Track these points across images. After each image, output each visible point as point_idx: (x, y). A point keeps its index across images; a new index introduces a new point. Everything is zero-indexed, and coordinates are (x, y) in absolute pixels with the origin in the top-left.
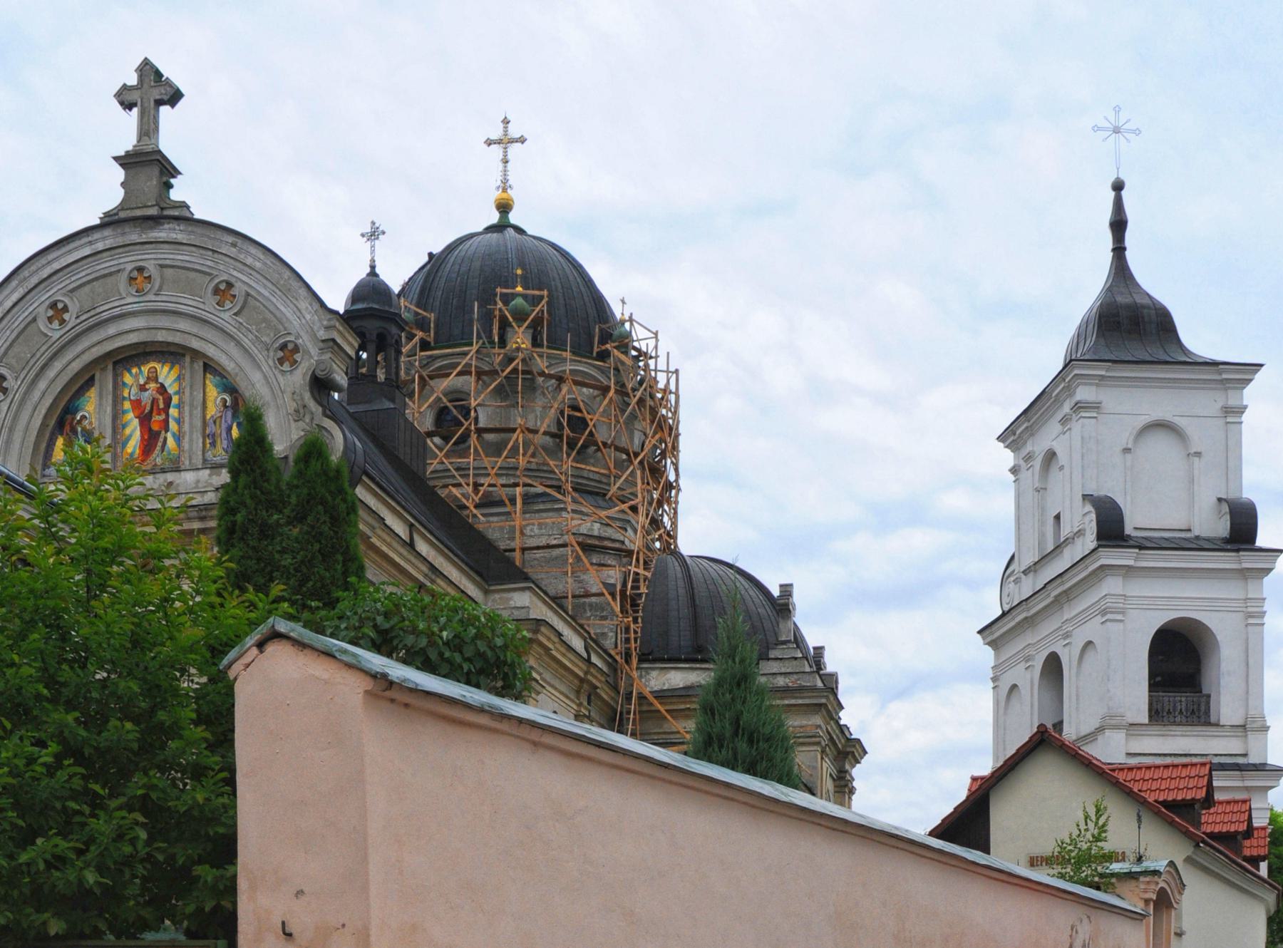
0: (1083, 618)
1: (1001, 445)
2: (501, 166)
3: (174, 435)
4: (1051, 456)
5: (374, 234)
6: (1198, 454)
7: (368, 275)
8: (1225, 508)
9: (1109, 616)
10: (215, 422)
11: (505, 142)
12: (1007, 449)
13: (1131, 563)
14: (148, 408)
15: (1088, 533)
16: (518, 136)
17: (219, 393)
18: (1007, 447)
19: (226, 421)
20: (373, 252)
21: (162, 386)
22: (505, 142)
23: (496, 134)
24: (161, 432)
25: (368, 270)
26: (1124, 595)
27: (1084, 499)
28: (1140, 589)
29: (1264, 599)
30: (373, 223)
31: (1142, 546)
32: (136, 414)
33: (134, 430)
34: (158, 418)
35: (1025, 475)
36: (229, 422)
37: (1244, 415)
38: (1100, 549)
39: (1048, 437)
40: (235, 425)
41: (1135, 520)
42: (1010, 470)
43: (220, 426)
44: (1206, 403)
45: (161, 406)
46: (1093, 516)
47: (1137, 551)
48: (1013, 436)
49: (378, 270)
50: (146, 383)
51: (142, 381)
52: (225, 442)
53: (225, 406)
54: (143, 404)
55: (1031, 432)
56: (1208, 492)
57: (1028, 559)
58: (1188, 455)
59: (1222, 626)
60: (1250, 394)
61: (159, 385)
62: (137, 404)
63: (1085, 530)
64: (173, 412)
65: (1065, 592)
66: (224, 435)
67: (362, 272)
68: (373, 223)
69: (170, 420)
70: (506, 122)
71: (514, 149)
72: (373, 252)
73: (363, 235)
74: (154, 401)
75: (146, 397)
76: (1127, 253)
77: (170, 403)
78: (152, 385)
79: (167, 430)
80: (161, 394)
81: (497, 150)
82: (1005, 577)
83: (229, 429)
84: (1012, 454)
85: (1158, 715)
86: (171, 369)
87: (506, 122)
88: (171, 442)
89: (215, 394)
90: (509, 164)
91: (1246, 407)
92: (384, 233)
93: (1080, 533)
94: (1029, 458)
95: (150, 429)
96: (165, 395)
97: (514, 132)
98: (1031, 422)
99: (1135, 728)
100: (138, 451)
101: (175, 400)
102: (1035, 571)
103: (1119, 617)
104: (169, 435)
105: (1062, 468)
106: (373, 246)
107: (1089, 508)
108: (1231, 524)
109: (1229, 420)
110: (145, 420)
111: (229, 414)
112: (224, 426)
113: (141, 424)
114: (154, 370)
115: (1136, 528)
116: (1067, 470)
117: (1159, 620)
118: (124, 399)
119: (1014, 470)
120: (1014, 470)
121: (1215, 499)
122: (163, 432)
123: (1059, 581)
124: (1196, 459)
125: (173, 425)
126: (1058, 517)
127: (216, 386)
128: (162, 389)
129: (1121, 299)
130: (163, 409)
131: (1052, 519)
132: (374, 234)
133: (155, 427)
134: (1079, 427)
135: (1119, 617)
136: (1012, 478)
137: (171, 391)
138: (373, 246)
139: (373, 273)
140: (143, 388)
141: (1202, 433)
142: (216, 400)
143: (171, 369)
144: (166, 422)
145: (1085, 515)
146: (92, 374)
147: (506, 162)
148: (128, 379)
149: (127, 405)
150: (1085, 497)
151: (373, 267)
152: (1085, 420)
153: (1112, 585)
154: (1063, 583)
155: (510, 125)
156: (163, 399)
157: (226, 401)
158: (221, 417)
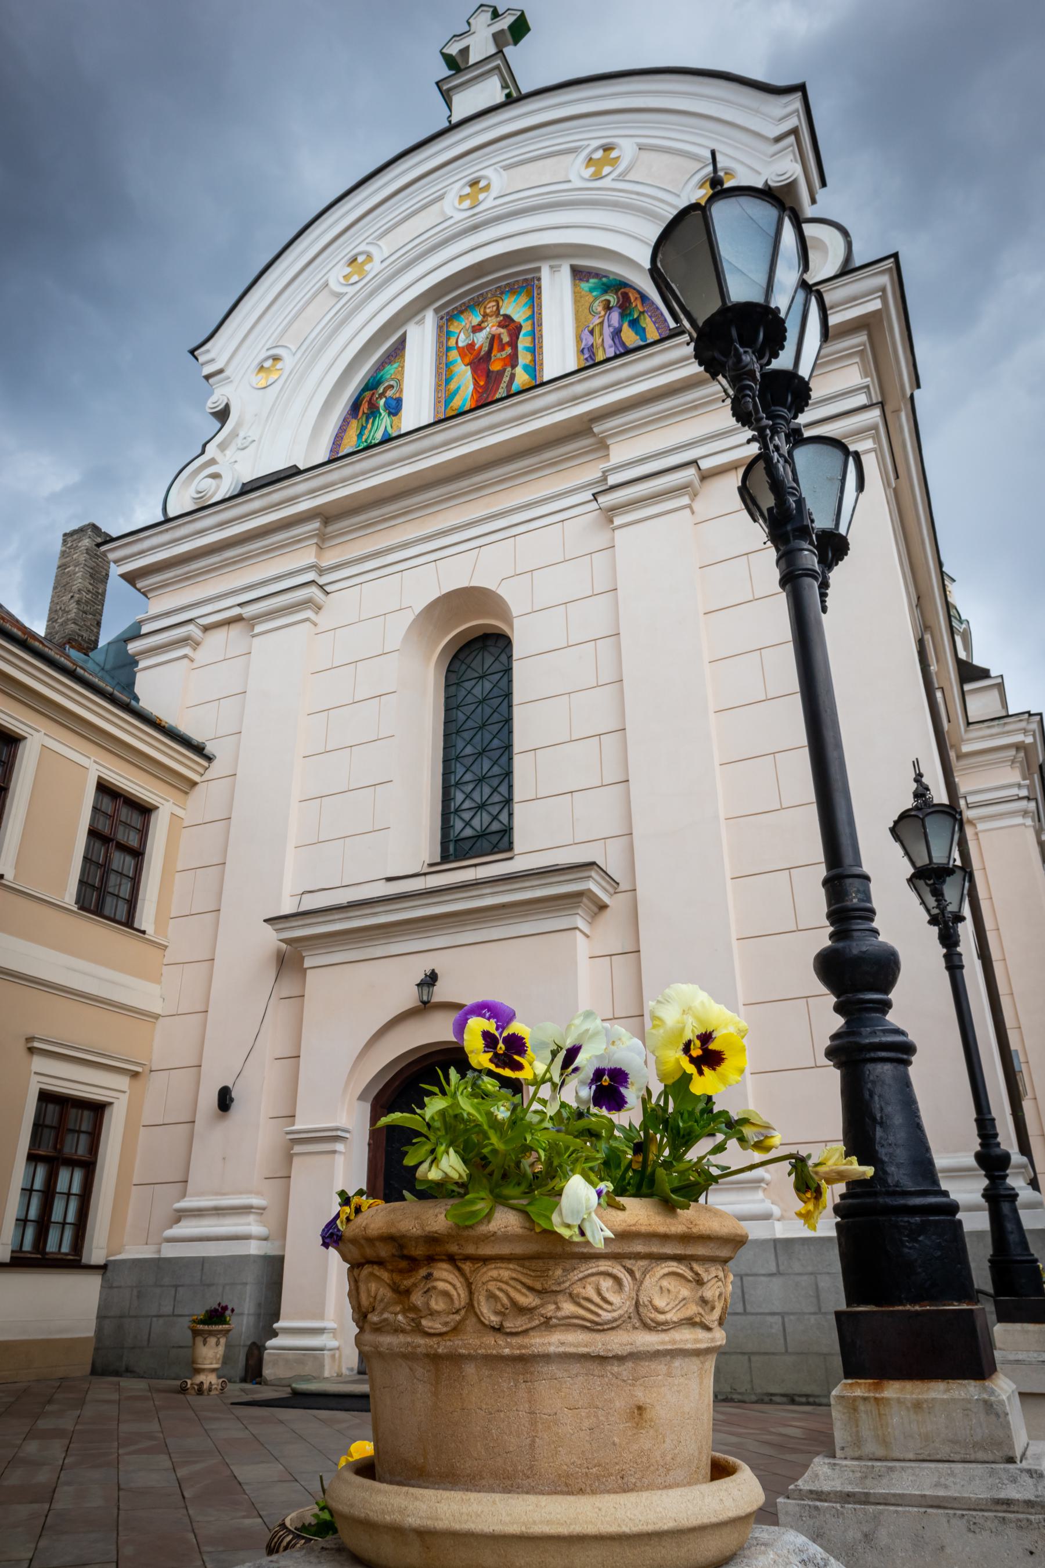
3: (526, 368)
14: (486, 348)
19: (609, 326)
21: (507, 317)
24: (504, 371)
32: (467, 360)
34: (499, 357)
40: (625, 326)
43: (601, 334)
45: (506, 339)
53: (608, 307)
54: (476, 347)
61: (501, 318)
74: (493, 339)
75: (481, 339)
78: (492, 321)
83: (617, 333)
95: (489, 374)
96: (512, 326)
101: (526, 328)
111: (615, 316)
112: (607, 331)
113: (474, 371)
122: (509, 369)
125: (524, 358)
128: (507, 321)
130: (508, 343)
133: (495, 367)
140: (477, 329)
149: (454, 355)
156: (508, 331)
157: (609, 302)
158: (602, 323)
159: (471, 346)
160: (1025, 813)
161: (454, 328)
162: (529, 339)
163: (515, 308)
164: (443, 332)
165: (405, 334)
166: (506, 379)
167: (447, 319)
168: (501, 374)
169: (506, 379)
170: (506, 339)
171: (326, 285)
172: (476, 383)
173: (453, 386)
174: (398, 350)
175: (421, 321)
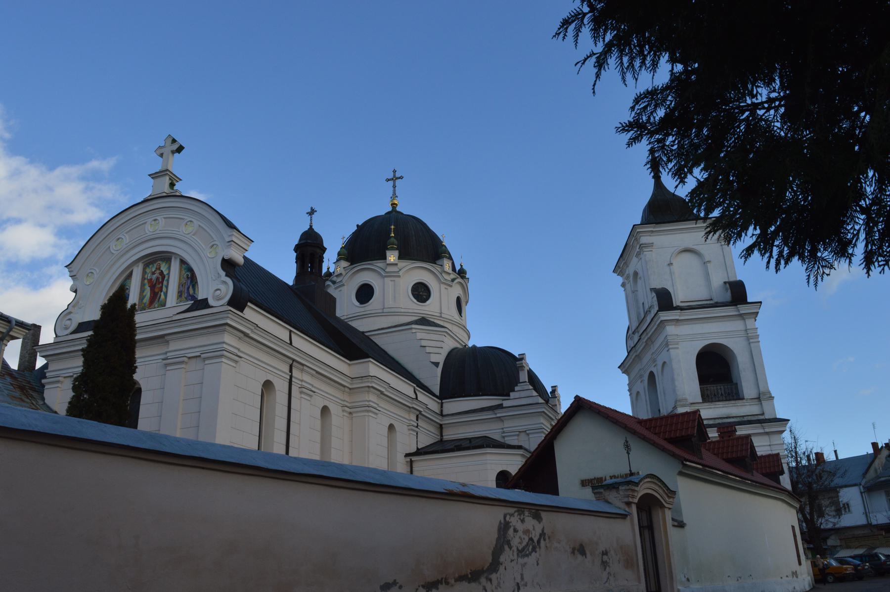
1: (616, 274)
2: (392, 189)
3: (164, 293)
4: (636, 274)
5: (312, 212)
6: (709, 262)
7: (309, 229)
8: (728, 285)
10: (182, 285)
11: (394, 179)
14: (155, 282)
15: (655, 307)
16: (400, 176)
17: (186, 272)
18: (618, 275)
20: (311, 220)
21: (162, 271)
22: (394, 179)
23: (391, 176)
25: (309, 227)
26: (677, 335)
27: (651, 291)
30: (312, 208)
31: (682, 309)
33: (148, 292)
35: (628, 286)
36: (189, 284)
38: (659, 313)
39: (634, 265)
40: (191, 287)
41: (679, 298)
42: (621, 286)
43: (185, 287)
45: (160, 280)
46: (655, 297)
47: (680, 311)
48: (619, 269)
49: (313, 227)
50: (155, 271)
51: (153, 270)
52: (186, 294)
53: (188, 278)
55: (627, 264)
56: (718, 279)
57: (634, 328)
62: (150, 281)
63: (654, 306)
64: (165, 283)
65: (649, 338)
66: (186, 291)
67: (307, 228)
68: (312, 208)
69: (164, 286)
70: (395, 171)
71: (398, 182)
72: (311, 220)
73: (307, 213)
74: (158, 278)
75: (154, 277)
77: (164, 279)
78: (158, 271)
79: (161, 291)
80: (161, 275)
81: (391, 183)
84: (621, 278)
85: (707, 397)
86: (166, 263)
87: (395, 171)
88: (163, 296)
89: (184, 273)
90: (396, 188)
92: (316, 211)
93: (651, 307)
94: (628, 277)
97: (398, 175)
99: (694, 405)
100: (148, 302)
101: (166, 278)
104: (162, 294)
105: (640, 278)
106: (311, 217)
107: (654, 294)
110: (152, 287)
111: (189, 281)
112: (186, 287)
113: (151, 290)
114: (159, 265)
115: (681, 302)
116: (642, 279)
118: (145, 279)
119: (623, 285)
120: (623, 285)
121: (722, 282)
123: (645, 334)
124: (709, 265)
125: (164, 289)
126: (643, 303)
127: (185, 269)
128: (162, 273)
130: (161, 282)
132: (312, 212)
133: (156, 290)
136: (623, 289)
137: (165, 273)
138: (311, 217)
139: (311, 226)
140: (153, 273)
142: (183, 276)
143: (166, 263)
144: (161, 288)
145: (652, 298)
146: (130, 270)
147: (394, 187)
148: (148, 270)
149: (146, 281)
150: (652, 290)
151: (311, 226)
154: (647, 334)
155: (396, 172)
159: (151, 279)
160: (368, 411)
161: (148, 270)
162: (166, 282)
163: (164, 268)
164: (144, 272)
165: (132, 270)
166: (159, 296)
167: (146, 265)
168: (158, 293)
169: (159, 296)
170: (160, 280)
171: (109, 247)
172: (151, 295)
173: (144, 294)
174: (130, 275)
175: (138, 266)
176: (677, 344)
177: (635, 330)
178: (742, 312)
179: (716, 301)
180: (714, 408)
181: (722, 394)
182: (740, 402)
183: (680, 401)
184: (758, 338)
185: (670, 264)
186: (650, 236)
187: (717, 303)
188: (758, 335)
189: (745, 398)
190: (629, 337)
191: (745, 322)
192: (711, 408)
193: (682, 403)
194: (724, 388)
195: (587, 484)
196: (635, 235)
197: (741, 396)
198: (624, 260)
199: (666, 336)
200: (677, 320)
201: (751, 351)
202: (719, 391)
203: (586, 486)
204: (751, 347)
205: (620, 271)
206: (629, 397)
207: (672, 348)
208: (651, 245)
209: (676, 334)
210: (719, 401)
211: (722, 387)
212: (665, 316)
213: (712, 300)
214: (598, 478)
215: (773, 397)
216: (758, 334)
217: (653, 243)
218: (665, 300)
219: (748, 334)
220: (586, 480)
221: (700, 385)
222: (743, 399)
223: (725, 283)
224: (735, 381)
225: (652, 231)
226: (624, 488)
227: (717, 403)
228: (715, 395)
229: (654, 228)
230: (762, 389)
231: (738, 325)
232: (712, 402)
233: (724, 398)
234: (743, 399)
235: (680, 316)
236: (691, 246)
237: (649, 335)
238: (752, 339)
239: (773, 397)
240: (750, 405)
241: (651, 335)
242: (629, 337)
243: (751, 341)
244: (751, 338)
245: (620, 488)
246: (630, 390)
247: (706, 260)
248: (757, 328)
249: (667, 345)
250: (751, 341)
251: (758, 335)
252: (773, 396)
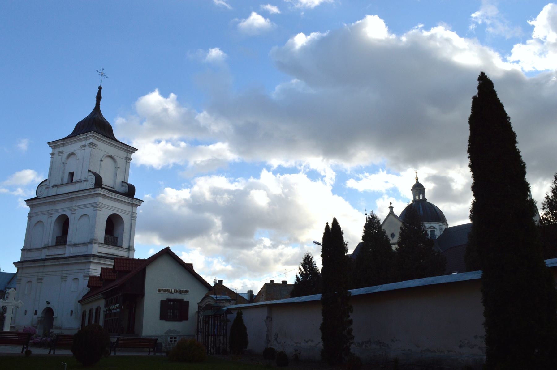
0: (86, 206)
1: (48, 145)
9: (98, 208)
12: (50, 148)
13: (106, 194)
26: (103, 203)
28: (106, 202)
29: (137, 213)
37: (131, 161)
44: (123, 154)
47: (108, 191)
56: (120, 179)
58: (116, 167)
59: (126, 218)
60: (133, 156)
65: (77, 197)
76: (100, 106)
82: (39, 186)
91: (132, 159)
98: (65, 142)
102: (58, 187)
103: (100, 209)
108: (128, 190)
109: (127, 161)
117: (111, 212)
120: (52, 154)
121: (121, 181)
123: (75, 193)
126: (72, 174)
129: (96, 116)
131: (68, 174)
134: (88, 150)
135: (100, 209)
136: (50, 156)
141: (121, 162)
150: (89, 171)
152: (92, 149)
153: (100, 199)
154: (77, 194)
176: (101, 208)
177: (57, 185)
178: (134, 203)
179: (116, 190)
180: (108, 248)
181: (110, 241)
182: (120, 249)
183: (95, 240)
184: (136, 218)
185: (101, 161)
186: (97, 140)
187: (116, 191)
188: (136, 217)
189: (123, 246)
190: (41, 186)
191: (133, 208)
192: (107, 248)
193: (95, 241)
194: (112, 238)
195: (161, 291)
196: (88, 135)
197: (118, 245)
198: (64, 142)
199: (98, 202)
200: (106, 195)
201: (131, 224)
202: (109, 239)
203: (161, 292)
204: (132, 222)
205: (55, 146)
206: (27, 221)
207: (98, 210)
208: (95, 145)
209: (102, 202)
210: (111, 245)
211: (111, 238)
212: (101, 191)
213: (114, 188)
214: (168, 289)
215: (135, 250)
216: (137, 216)
217: (97, 145)
218: (99, 182)
219: (132, 214)
220: (161, 289)
221: (105, 234)
222: (121, 247)
223: (122, 182)
224: (115, 235)
225: (99, 138)
226: (233, 302)
227: (111, 246)
228: (110, 241)
229: (101, 137)
230: (131, 245)
231: (128, 208)
232: (109, 245)
233: (110, 244)
234: (121, 247)
235: (108, 194)
236: (113, 155)
237: (78, 196)
238: (133, 218)
239: (135, 250)
240: (124, 251)
241: (78, 196)
242: (41, 186)
243: (133, 219)
244: (133, 216)
245: (232, 302)
246: (30, 217)
247: (118, 166)
248: (137, 213)
249: (96, 207)
250: (133, 219)
251: (136, 217)
252: (135, 249)
